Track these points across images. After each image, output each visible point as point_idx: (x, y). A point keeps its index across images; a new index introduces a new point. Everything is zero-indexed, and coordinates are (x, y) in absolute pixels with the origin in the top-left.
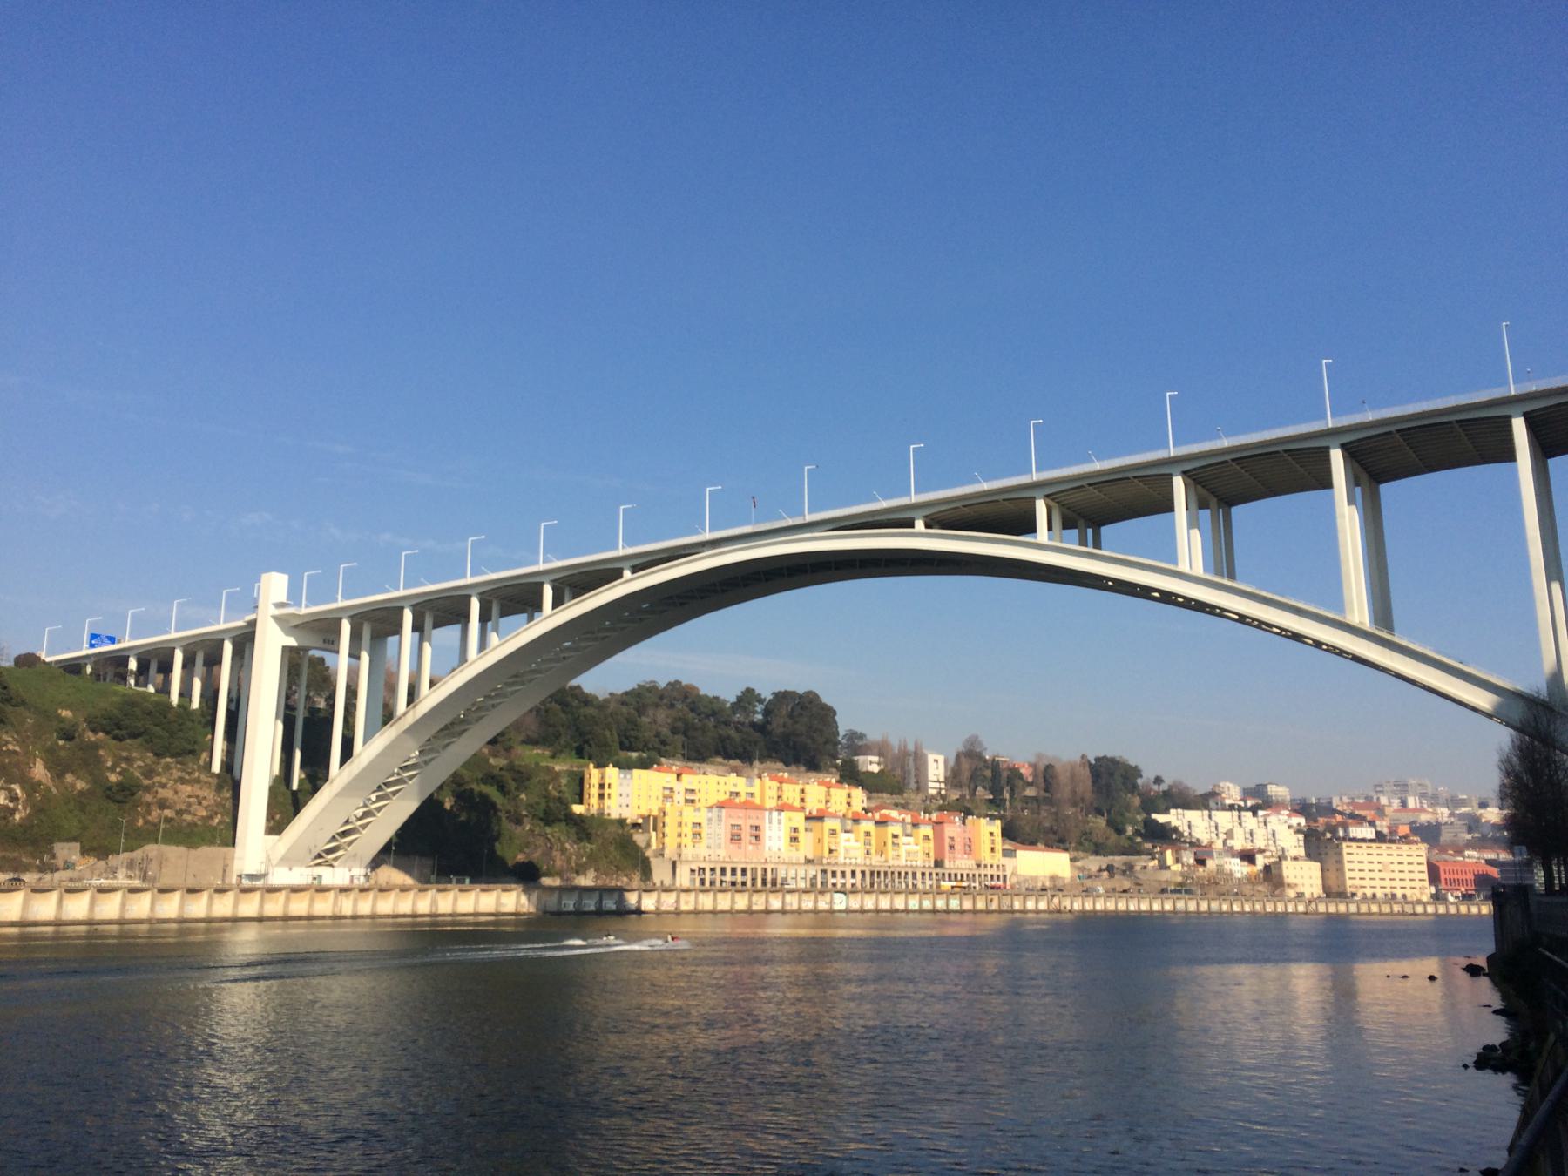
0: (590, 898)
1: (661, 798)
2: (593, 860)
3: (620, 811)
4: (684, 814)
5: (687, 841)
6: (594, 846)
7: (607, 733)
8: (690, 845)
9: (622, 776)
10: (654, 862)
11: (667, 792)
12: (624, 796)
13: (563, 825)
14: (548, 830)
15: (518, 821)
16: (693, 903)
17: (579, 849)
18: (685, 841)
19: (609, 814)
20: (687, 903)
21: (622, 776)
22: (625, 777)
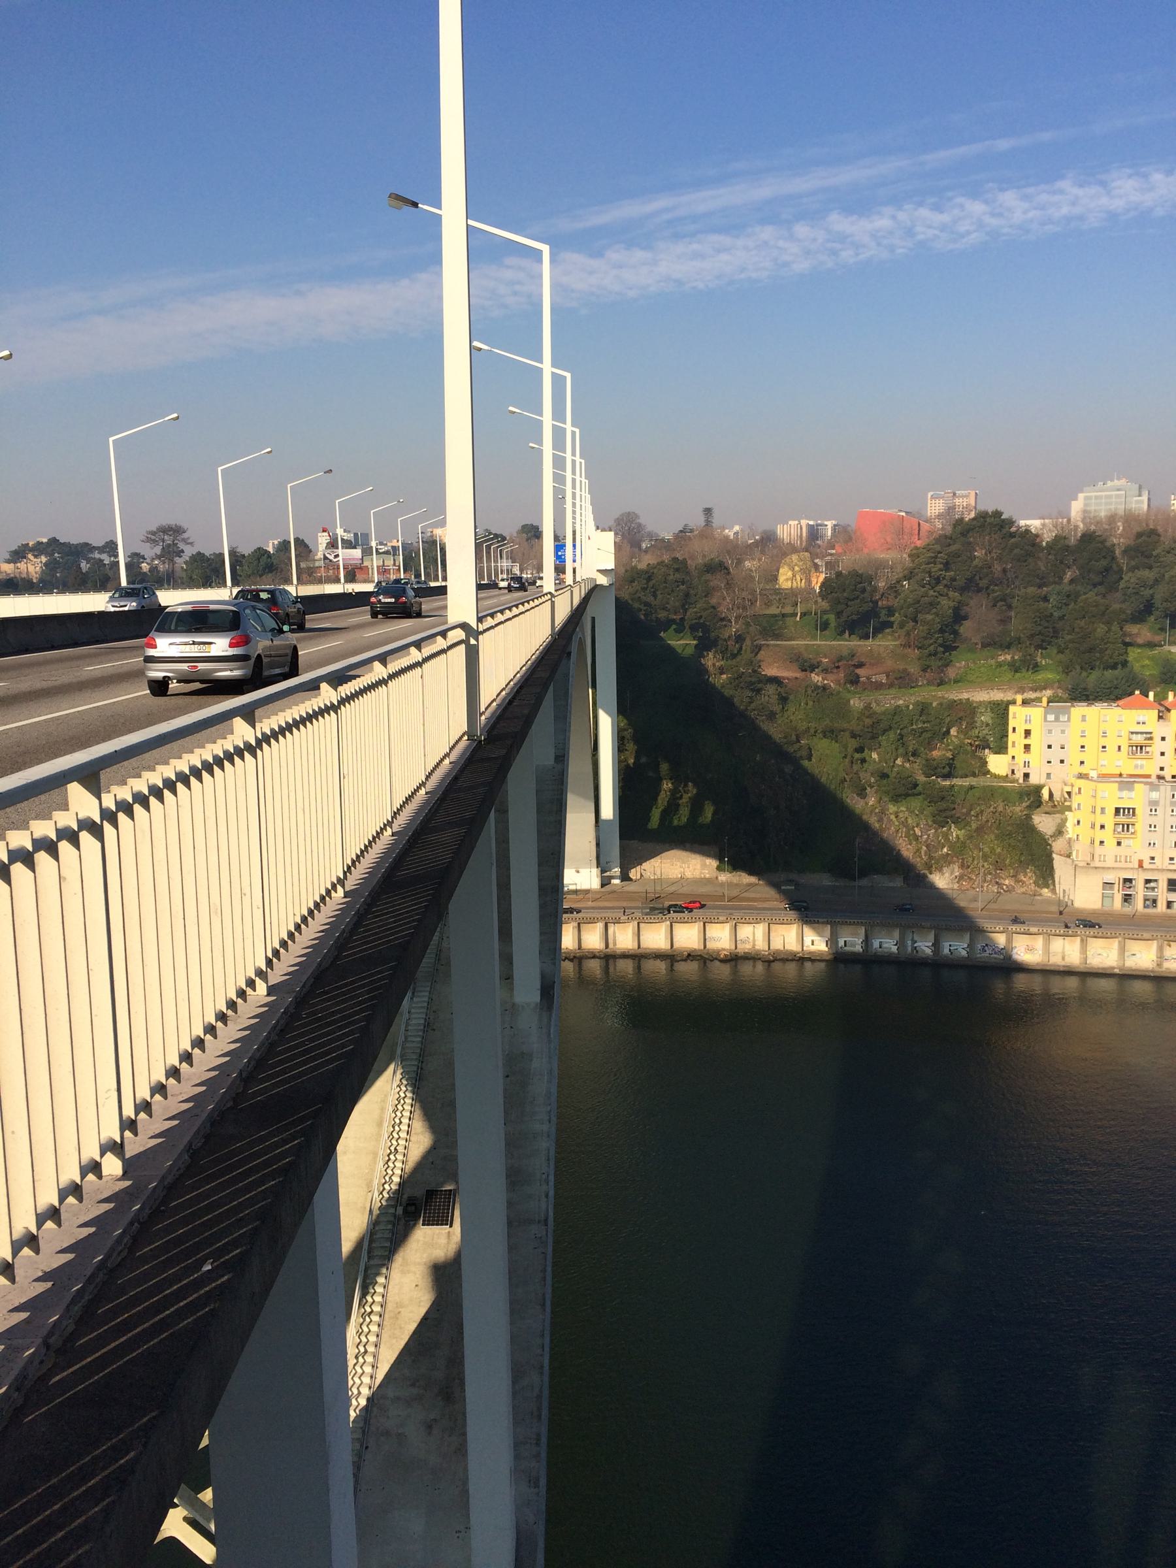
0: (855, 935)
1: (1124, 748)
2: (959, 851)
3: (1047, 769)
4: (1099, 794)
5: (1108, 836)
6: (961, 833)
7: (1101, 629)
8: (1110, 842)
9: (1051, 717)
10: (1058, 862)
11: (1139, 739)
12: (1056, 747)
13: (916, 803)
14: (892, 808)
15: (862, 793)
16: (1041, 952)
17: (936, 835)
18: (1100, 835)
19: (1026, 776)
20: (1030, 949)
21: (1051, 717)
22: (1057, 719)
